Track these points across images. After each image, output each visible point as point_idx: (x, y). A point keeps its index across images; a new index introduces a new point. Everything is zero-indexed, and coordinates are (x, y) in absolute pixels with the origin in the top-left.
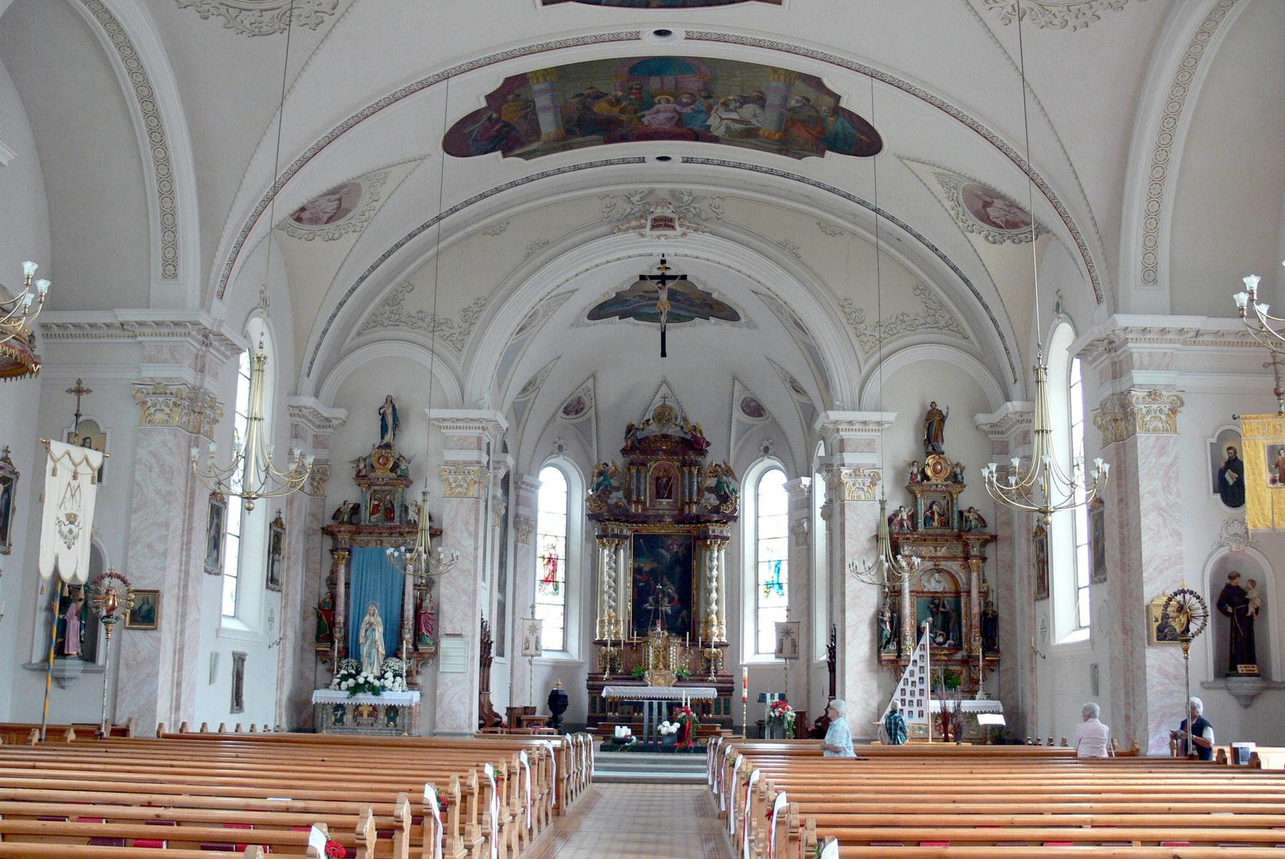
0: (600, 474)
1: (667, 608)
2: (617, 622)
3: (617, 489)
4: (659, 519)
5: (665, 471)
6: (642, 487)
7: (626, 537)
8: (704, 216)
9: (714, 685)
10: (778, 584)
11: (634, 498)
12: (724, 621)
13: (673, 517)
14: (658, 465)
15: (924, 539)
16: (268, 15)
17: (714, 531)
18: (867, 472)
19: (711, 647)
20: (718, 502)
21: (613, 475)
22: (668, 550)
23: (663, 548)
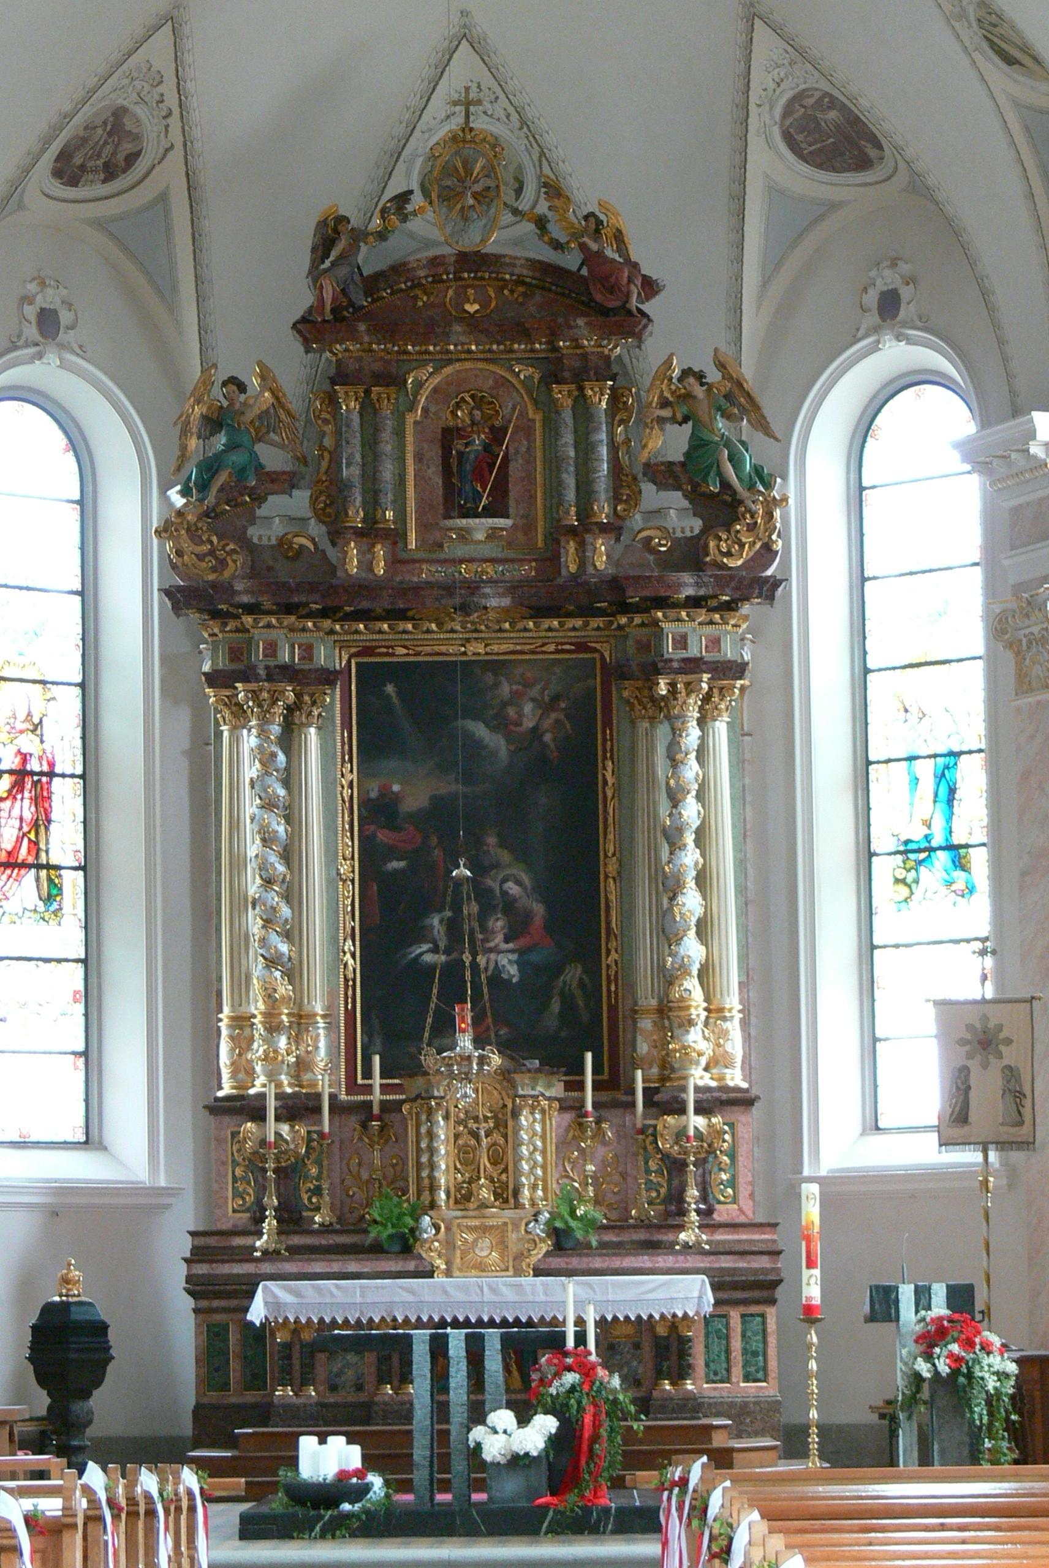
0: (214, 422)
1: (503, 960)
2: (302, 1021)
3: (286, 482)
5: (479, 402)
6: (387, 472)
7: (328, 677)
9: (693, 1261)
10: (950, 847)
11: (356, 517)
12: (733, 1002)
13: (514, 588)
14: (448, 382)
17: (682, 642)
19: (682, 1110)
20: (696, 525)
21: (267, 423)
22: (500, 723)
23: (476, 717)
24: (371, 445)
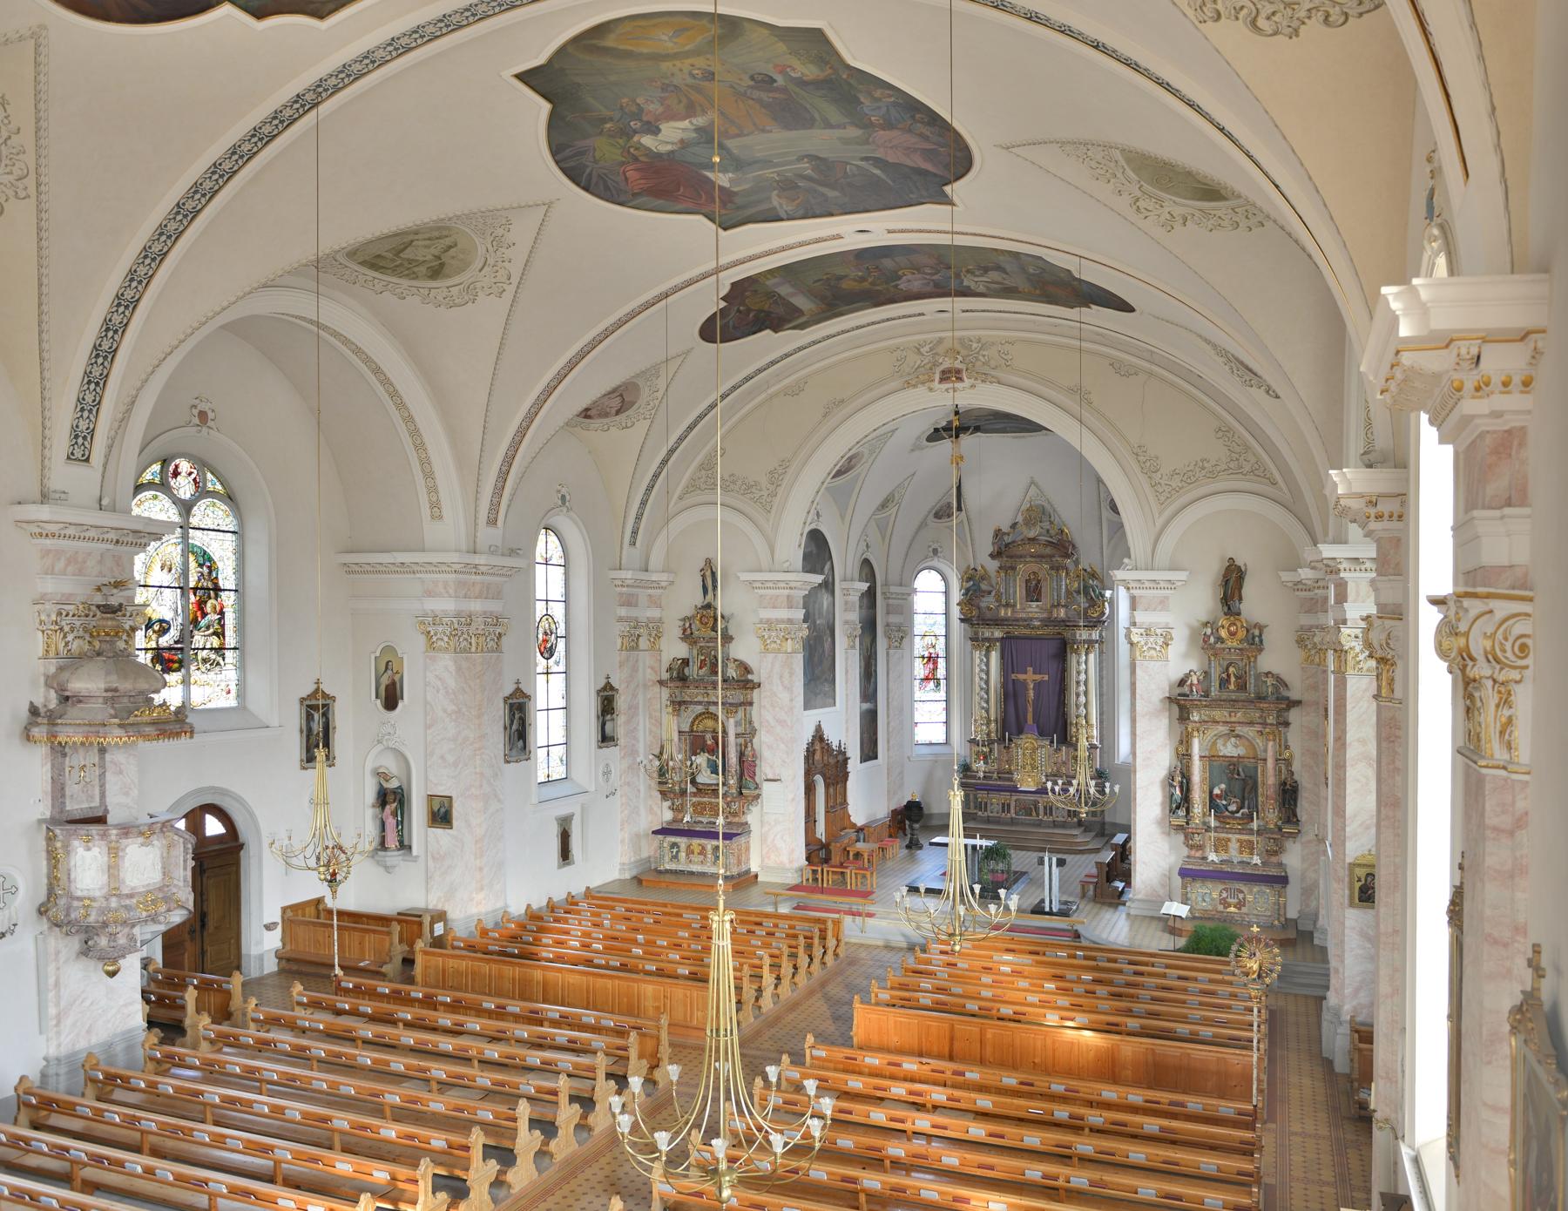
0: (969, 579)
4: (1027, 622)
8: (993, 363)
15: (1217, 703)
16: (455, 290)
17: (1081, 635)
18: (1159, 632)
21: (983, 578)
24: (1007, 584)
